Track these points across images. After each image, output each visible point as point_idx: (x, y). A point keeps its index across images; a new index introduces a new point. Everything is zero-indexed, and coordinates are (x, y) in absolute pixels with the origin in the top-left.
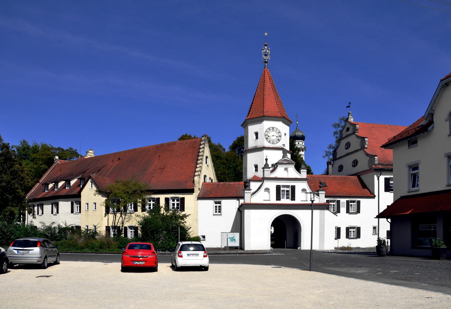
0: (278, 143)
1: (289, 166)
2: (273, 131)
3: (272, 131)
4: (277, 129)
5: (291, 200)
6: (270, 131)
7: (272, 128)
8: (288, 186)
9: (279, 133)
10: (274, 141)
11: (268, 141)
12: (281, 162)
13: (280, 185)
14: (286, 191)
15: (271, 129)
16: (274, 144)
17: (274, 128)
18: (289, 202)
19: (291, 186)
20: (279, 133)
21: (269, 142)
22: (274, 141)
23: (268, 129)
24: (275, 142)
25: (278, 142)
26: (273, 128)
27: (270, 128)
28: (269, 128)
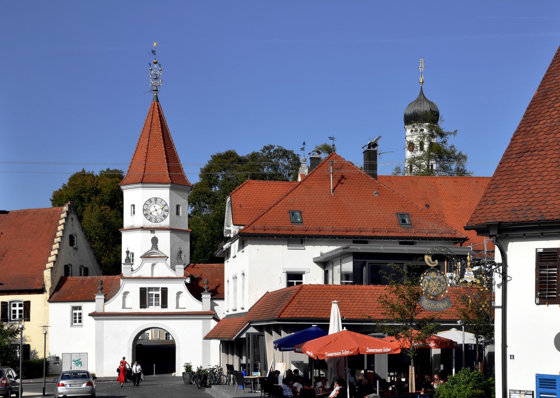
0: (163, 220)
1: (159, 261)
2: (156, 203)
3: (154, 203)
4: (162, 200)
5: (162, 308)
6: (152, 204)
7: (154, 199)
8: (157, 289)
9: (164, 206)
10: (158, 218)
11: (148, 219)
12: (147, 256)
13: (146, 288)
14: (155, 295)
15: (153, 200)
16: (157, 222)
17: (158, 199)
18: (158, 309)
19: (162, 288)
20: (164, 206)
21: (149, 220)
22: (158, 218)
23: (148, 201)
24: (159, 220)
25: (163, 219)
26: (156, 199)
27: (151, 199)
28: (150, 199)
